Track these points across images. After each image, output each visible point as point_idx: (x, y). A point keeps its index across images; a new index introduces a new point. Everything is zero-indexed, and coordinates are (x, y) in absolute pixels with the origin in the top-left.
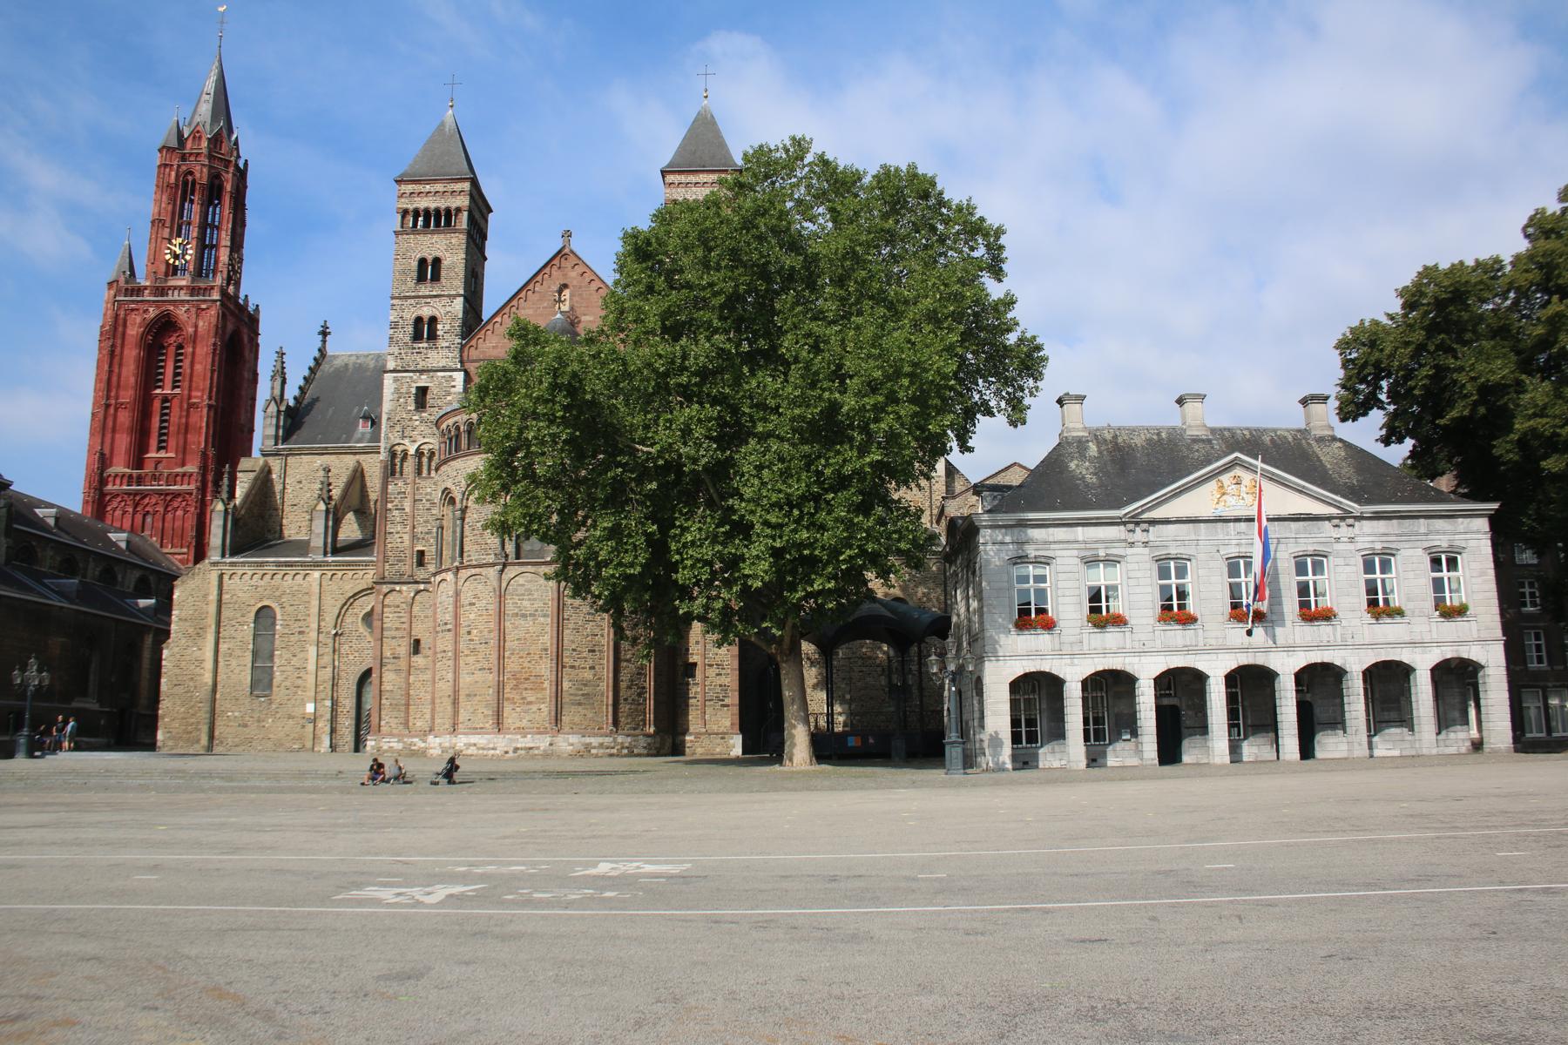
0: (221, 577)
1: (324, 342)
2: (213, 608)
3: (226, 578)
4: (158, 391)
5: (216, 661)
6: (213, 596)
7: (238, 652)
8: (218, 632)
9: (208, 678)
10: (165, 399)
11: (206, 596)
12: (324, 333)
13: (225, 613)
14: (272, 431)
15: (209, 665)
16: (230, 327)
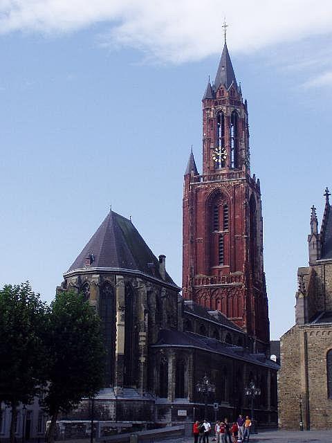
0: (305, 333)
1: (328, 199)
2: (302, 351)
3: (308, 334)
4: (216, 231)
5: (307, 381)
6: (302, 345)
7: (319, 375)
8: (307, 364)
9: (303, 388)
10: (221, 236)
11: (298, 345)
12: (327, 195)
13: (310, 353)
14: (315, 252)
15: (303, 382)
16: (250, 193)
